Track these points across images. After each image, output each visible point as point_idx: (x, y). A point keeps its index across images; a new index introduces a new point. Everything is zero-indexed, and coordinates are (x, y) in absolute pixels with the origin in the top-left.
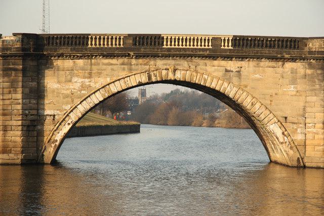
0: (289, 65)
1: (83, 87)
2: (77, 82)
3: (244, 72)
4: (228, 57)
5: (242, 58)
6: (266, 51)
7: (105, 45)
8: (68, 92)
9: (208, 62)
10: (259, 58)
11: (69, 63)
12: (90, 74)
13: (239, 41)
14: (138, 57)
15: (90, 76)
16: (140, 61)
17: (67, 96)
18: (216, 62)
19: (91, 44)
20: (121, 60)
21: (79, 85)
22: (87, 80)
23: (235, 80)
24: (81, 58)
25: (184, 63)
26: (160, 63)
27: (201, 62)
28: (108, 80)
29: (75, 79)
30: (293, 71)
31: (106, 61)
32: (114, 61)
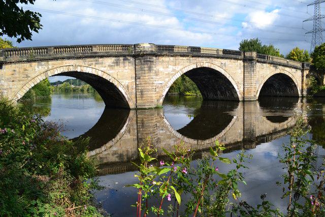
0: (239, 62)
1: (174, 70)
2: (171, 68)
3: (227, 64)
4: (222, 58)
5: (227, 58)
6: (233, 56)
7: (181, 50)
8: (167, 72)
9: (216, 59)
10: (231, 58)
11: (166, 59)
12: (175, 64)
13: (225, 52)
14: (193, 57)
15: (175, 65)
16: (193, 58)
17: (167, 74)
18: (218, 60)
19: (176, 50)
20: (187, 58)
21: (171, 69)
22: (174, 67)
23: (224, 68)
24: (172, 56)
25: (208, 60)
26: (200, 59)
27: (214, 59)
28: (182, 67)
29: (170, 66)
30: (240, 64)
31: (181, 58)
32: (184, 58)
